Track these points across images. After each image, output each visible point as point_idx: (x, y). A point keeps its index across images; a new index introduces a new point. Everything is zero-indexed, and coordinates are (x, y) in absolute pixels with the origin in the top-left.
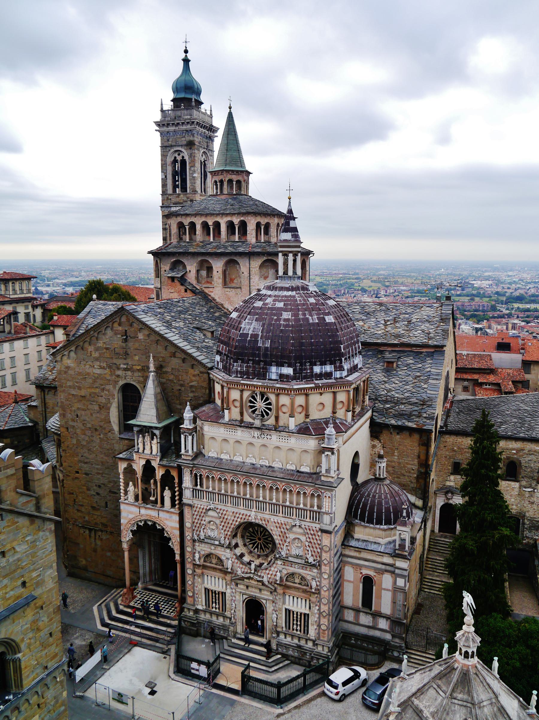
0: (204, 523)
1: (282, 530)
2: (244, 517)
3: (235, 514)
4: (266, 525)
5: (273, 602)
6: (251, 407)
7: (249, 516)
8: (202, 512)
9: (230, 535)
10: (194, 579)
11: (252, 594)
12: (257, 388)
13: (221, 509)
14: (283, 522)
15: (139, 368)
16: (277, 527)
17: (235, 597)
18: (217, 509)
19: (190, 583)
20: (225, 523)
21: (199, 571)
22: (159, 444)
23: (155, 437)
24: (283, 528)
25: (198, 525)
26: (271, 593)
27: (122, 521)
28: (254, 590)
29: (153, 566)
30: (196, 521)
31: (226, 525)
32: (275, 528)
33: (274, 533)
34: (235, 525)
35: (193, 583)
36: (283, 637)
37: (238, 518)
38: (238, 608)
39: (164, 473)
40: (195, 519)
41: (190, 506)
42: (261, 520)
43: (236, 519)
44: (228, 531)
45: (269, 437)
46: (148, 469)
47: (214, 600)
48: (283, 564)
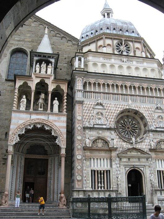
0: (93, 114)
1: (150, 112)
2: (123, 107)
3: (116, 106)
4: (139, 110)
5: (149, 167)
6: (117, 49)
7: (127, 106)
8: (90, 107)
9: (113, 121)
10: (83, 163)
11: (133, 164)
12: (123, 38)
13: (106, 103)
14: (149, 107)
15: (30, 40)
16: (145, 110)
17: (120, 171)
18: (103, 103)
19: (79, 167)
20: (109, 113)
21: (88, 154)
22: (53, 68)
23: (50, 64)
24: (150, 111)
25: (87, 117)
26: (147, 159)
27: (12, 127)
28: (134, 159)
29: (18, 186)
30: (86, 114)
31: (110, 114)
32: (145, 111)
33: (144, 115)
34: (116, 113)
35: (82, 167)
36: (160, 194)
37: (119, 108)
38: (122, 180)
39: (55, 87)
40: (85, 113)
41: (81, 103)
42: (135, 107)
43: (117, 109)
44: (112, 118)
45: (131, 62)
46: (42, 86)
47: (99, 180)
48: (153, 135)
